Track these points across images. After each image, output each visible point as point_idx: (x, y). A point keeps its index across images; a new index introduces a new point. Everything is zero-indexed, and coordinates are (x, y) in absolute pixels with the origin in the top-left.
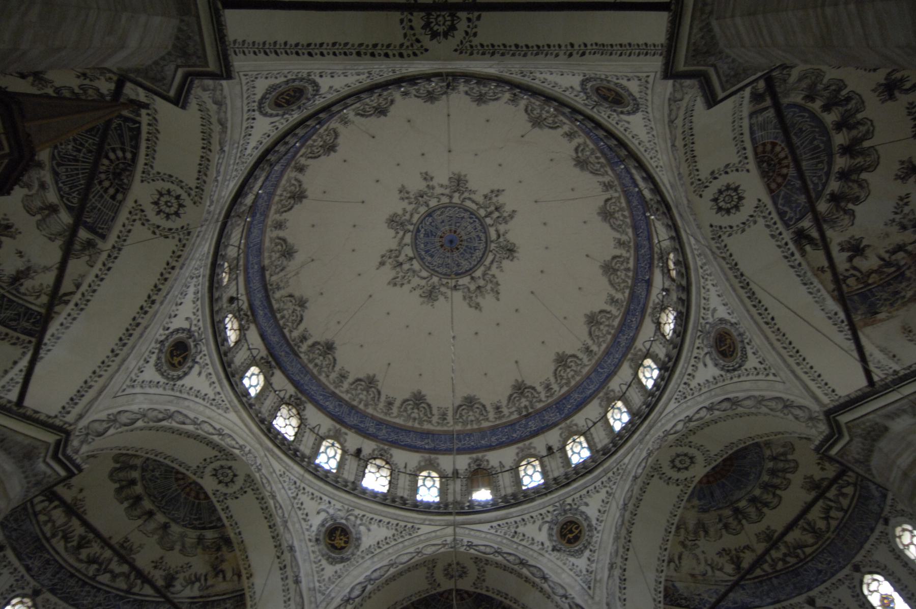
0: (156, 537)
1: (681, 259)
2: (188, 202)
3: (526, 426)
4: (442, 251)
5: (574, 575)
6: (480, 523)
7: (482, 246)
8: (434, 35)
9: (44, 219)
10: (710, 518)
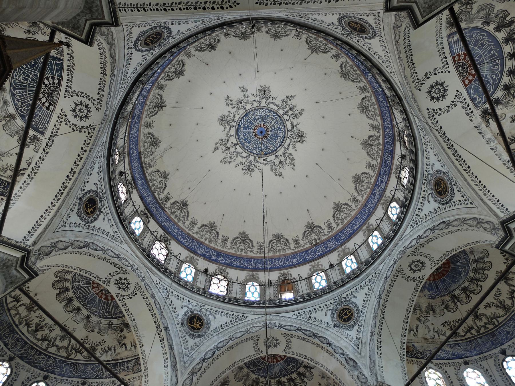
0: (83, 324)
1: (411, 133)
2: (93, 109)
3: (315, 251)
4: (255, 138)
5: (348, 341)
6: (287, 312)
7: (282, 134)
9: (7, 123)
10: (436, 302)
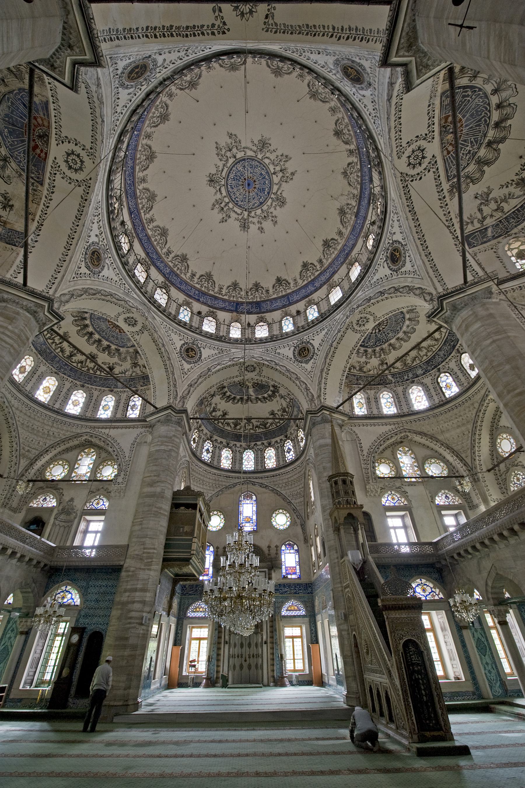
2: (355, 322)
4: (255, 178)
7: (230, 181)
8: (253, 366)
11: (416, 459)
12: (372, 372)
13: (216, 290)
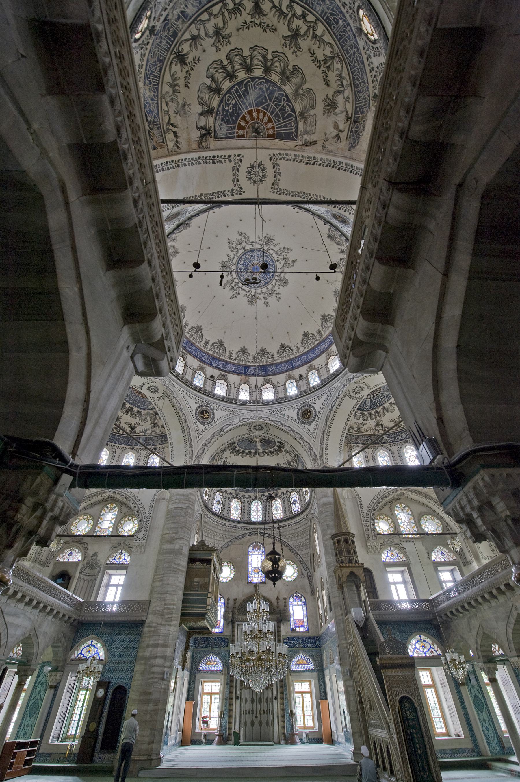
7: (239, 266)
11: (413, 515)
12: (369, 433)
13: (227, 355)
